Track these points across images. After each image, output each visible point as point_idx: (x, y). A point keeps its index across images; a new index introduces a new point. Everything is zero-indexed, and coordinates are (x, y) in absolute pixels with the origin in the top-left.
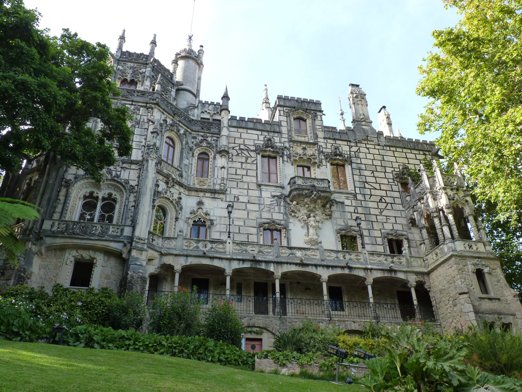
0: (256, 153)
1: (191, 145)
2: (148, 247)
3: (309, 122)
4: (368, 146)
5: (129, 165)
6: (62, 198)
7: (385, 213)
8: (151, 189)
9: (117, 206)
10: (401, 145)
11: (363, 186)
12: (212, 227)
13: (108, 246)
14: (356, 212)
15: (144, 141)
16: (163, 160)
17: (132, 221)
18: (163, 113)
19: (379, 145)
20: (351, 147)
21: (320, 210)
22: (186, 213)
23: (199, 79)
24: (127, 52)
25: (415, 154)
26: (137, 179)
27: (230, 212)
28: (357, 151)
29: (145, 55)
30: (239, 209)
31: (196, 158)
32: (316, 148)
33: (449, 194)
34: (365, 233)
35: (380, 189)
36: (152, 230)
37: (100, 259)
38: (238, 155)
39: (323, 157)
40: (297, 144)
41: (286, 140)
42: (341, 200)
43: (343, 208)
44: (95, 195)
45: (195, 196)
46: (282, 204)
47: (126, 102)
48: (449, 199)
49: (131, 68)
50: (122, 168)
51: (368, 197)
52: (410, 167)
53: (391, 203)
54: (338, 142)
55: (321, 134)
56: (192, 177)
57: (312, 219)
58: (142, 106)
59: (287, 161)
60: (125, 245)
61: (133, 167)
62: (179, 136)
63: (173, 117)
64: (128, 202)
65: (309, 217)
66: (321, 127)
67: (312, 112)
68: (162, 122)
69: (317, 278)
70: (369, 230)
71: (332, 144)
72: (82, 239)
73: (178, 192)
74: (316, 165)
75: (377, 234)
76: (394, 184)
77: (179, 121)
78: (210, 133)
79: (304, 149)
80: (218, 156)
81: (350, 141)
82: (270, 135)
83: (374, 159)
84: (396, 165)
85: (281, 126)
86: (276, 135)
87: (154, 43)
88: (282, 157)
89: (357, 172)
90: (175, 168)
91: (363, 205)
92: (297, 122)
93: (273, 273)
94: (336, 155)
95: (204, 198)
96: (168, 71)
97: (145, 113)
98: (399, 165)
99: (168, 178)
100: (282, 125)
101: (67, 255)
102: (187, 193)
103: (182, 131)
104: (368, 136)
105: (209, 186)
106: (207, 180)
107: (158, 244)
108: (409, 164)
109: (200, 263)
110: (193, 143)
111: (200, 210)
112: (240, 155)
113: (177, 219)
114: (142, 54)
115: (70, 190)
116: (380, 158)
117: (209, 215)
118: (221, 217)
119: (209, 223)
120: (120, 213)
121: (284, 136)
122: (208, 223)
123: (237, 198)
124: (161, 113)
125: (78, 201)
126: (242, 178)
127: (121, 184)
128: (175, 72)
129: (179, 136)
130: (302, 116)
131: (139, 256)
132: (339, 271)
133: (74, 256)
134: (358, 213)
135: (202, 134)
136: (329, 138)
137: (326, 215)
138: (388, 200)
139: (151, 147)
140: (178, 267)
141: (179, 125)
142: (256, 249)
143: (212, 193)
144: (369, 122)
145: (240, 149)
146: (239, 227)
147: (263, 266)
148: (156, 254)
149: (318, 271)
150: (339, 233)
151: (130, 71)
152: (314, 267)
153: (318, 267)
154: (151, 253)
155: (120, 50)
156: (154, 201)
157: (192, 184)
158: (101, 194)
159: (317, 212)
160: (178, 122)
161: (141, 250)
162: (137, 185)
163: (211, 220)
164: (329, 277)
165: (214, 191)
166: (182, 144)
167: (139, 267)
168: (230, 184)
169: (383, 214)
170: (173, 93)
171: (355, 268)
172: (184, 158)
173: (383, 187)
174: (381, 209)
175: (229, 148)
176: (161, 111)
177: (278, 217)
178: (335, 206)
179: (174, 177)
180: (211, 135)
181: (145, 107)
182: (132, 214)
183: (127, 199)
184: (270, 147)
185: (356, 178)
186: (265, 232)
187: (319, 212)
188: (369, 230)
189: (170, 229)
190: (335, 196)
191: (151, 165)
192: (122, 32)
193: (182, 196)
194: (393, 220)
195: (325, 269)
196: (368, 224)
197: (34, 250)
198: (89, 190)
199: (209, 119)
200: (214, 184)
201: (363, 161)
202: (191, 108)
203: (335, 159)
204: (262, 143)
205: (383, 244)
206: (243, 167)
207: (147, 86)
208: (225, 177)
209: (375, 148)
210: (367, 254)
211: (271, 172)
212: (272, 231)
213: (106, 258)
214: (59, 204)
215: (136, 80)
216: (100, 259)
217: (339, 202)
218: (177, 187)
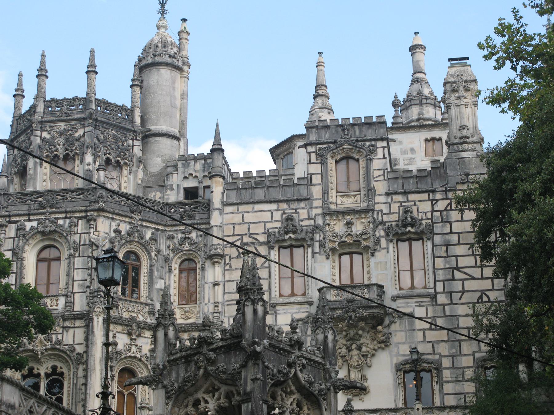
3: (362, 163)
5: (73, 321)
8: (101, 360)
11: (450, 277)
15: (89, 279)
18: (113, 219)
20: (434, 202)
21: (368, 336)
23: (184, 96)
24: (52, 100)
26: (85, 343)
28: (445, 210)
29: (81, 99)
31: (177, 272)
34: (446, 363)
35: (482, 278)
39: (383, 233)
40: (337, 216)
41: (319, 211)
42: (406, 310)
43: (412, 324)
44: (35, 371)
47: (57, 216)
49: (61, 134)
50: (64, 328)
51: (456, 296)
54: (412, 197)
55: (381, 187)
57: (355, 352)
59: (319, 253)
61: (78, 323)
62: (145, 246)
63: (131, 218)
64: (77, 378)
65: (349, 350)
66: (381, 172)
67: (368, 144)
68: (113, 235)
70: (453, 356)
71: (401, 202)
77: (142, 220)
79: (349, 224)
80: (208, 264)
82: (292, 207)
85: (312, 184)
86: (302, 205)
87: (91, 71)
88: (311, 246)
89: (442, 251)
90: (142, 303)
91: (448, 313)
92: (343, 165)
94: (405, 226)
97: (86, 228)
99: (131, 326)
100: (314, 182)
103: (148, 235)
104: (467, 175)
105: (198, 318)
106: (195, 308)
110: (169, 247)
114: (74, 99)
120: (69, 394)
121: (316, 203)
124: (109, 221)
127: (65, 353)
129: (143, 246)
130: (350, 154)
136: (396, 193)
137: (380, 343)
139: (96, 294)
141: (142, 225)
150: (400, 370)
151: (61, 141)
158: (43, 369)
160: (140, 223)
162: (86, 352)
166: (150, 256)
170: (137, 151)
176: (109, 218)
179: (141, 318)
182: (83, 397)
183: (76, 374)
185: (440, 263)
187: (366, 339)
191: (98, 323)
196: (452, 347)
201: (456, 227)
202: (169, 170)
204: (279, 225)
207: (89, 164)
208: (220, 299)
217: (404, 314)
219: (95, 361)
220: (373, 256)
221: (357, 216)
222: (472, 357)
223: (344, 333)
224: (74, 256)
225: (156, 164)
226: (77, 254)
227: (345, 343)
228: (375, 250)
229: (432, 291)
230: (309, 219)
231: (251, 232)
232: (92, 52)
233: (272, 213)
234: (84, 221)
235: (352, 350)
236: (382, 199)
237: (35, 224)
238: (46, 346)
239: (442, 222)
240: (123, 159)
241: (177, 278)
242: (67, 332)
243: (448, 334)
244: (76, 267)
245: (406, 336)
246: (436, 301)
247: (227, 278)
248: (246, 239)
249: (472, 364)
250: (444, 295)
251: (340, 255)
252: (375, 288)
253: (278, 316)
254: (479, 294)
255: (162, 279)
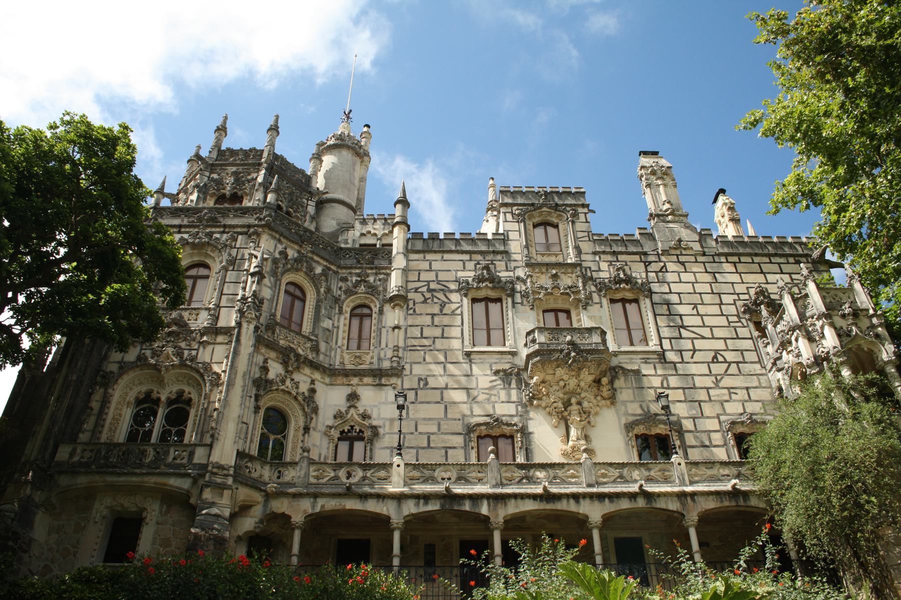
0: (461, 296)
1: (337, 292)
2: (235, 481)
4: (682, 259)
6: (95, 405)
7: (727, 382)
8: (244, 375)
9: (192, 412)
10: (748, 250)
11: (676, 335)
12: (375, 441)
13: (165, 485)
14: (665, 385)
16: (277, 324)
17: (212, 436)
18: (279, 241)
19: (704, 254)
20: (647, 264)
22: (326, 417)
23: (363, 180)
24: (228, 149)
25: (779, 264)
27: (400, 407)
28: (661, 271)
29: (258, 151)
30: (428, 403)
31: (348, 315)
32: (579, 273)
33: (838, 326)
34: (688, 425)
35: (713, 338)
36: (254, 452)
37: (153, 511)
38: (425, 301)
39: (593, 288)
44: (154, 395)
45: (343, 385)
46: (514, 385)
47: (213, 230)
48: (839, 336)
50: (200, 343)
51: (687, 356)
52: (772, 289)
53: (738, 363)
54: (621, 257)
56: (339, 350)
58: (241, 233)
59: (522, 304)
60: (195, 481)
61: (220, 339)
62: (315, 280)
63: (301, 246)
66: (586, 234)
67: (568, 209)
68: (277, 256)
69: (582, 522)
70: (694, 419)
71: (611, 262)
72: (119, 475)
73: (309, 380)
74: (581, 305)
75: (713, 425)
76: (739, 324)
77: (313, 252)
78: (372, 269)
79: (555, 277)
80: (387, 308)
81: (645, 254)
83: (697, 282)
84: (740, 288)
85: (508, 240)
86: (499, 257)
87: (274, 129)
90: (304, 336)
92: (540, 231)
93: (487, 519)
95: (359, 388)
96: (302, 172)
98: (748, 288)
100: (511, 238)
101: (97, 505)
102: (327, 380)
103: (319, 270)
105: (371, 363)
107: (261, 476)
108: (767, 283)
109: (340, 507)
111: (352, 411)
112: (429, 301)
113: (307, 429)
115: (110, 391)
116: (708, 278)
117: (369, 417)
118: (392, 420)
119: (370, 433)
122: (368, 434)
123: (423, 381)
125: (124, 410)
126: (434, 342)
127: (198, 371)
128: (315, 174)
130: (549, 218)
131: (217, 500)
132: (625, 504)
133: (107, 507)
134: (669, 388)
135: (358, 271)
137: (604, 399)
138: (730, 356)
140: (298, 518)
141: (312, 259)
142: (454, 475)
143: (375, 376)
144: (681, 215)
145: (429, 290)
146: (429, 435)
147: (467, 506)
148: (258, 497)
149: (582, 507)
151: (231, 180)
152: (572, 501)
153: (581, 501)
154: (244, 493)
155: (217, 149)
156: (257, 398)
157: (337, 363)
159: (583, 395)
160: (310, 255)
161: (221, 488)
163: (375, 429)
164: (607, 519)
165: (378, 372)
167: (213, 519)
168: (409, 357)
169: (721, 385)
170: (311, 209)
171: (659, 495)
172: (322, 318)
173: (718, 333)
174: (716, 375)
175: (408, 291)
176: (274, 238)
177: (506, 409)
178: (622, 379)
179: (300, 352)
180: (374, 271)
181: (246, 233)
184: (486, 280)
185: (662, 321)
186: (480, 441)
188: (694, 419)
189: (294, 449)
190: (622, 360)
192: (222, 119)
193: (319, 387)
194: (742, 394)
195: (596, 503)
197: (37, 499)
198: (144, 389)
199: (375, 245)
200: (379, 359)
201: (675, 288)
203: (617, 289)
204: (472, 274)
205: (725, 444)
206: (436, 323)
208: (401, 344)
209: (696, 262)
210: (683, 464)
211: (491, 326)
212: (495, 439)
213: (165, 507)
214: (89, 415)
215: (240, 193)
216: (153, 511)
218: (307, 371)
219: (236, 374)
220: (585, 309)
221: (563, 271)
222: (716, 420)
223: (562, 383)
224: (227, 270)
225: (329, 224)
226: (231, 268)
227: (562, 396)
228: (587, 304)
229: (658, 348)
230: (507, 270)
231: (439, 279)
232: (277, 117)
233: (464, 263)
234: (245, 236)
235: (571, 404)
236: (590, 257)
237: (186, 236)
238: (173, 361)
239: (659, 282)
240: (295, 212)
241: (347, 322)
242: (204, 348)
243: (684, 394)
244: (227, 280)
245: (634, 394)
246: (664, 358)
247: (410, 323)
248: (433, 286)
249: (718, 428)
250: (673, 353)
251: (544, 311)
252: (599, 332)
253: (473, 365)
254: (713, 354)
255: (330, 319)
